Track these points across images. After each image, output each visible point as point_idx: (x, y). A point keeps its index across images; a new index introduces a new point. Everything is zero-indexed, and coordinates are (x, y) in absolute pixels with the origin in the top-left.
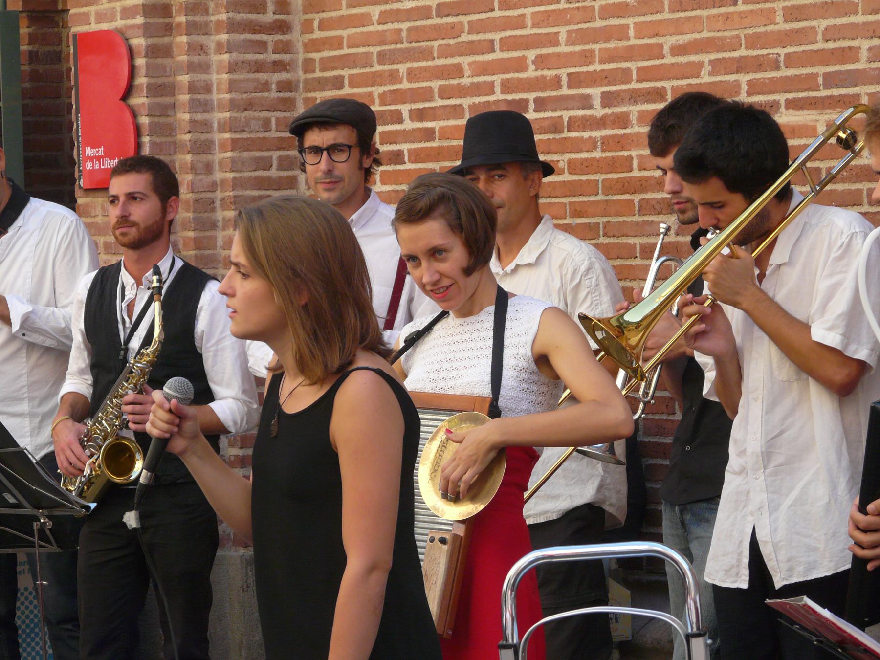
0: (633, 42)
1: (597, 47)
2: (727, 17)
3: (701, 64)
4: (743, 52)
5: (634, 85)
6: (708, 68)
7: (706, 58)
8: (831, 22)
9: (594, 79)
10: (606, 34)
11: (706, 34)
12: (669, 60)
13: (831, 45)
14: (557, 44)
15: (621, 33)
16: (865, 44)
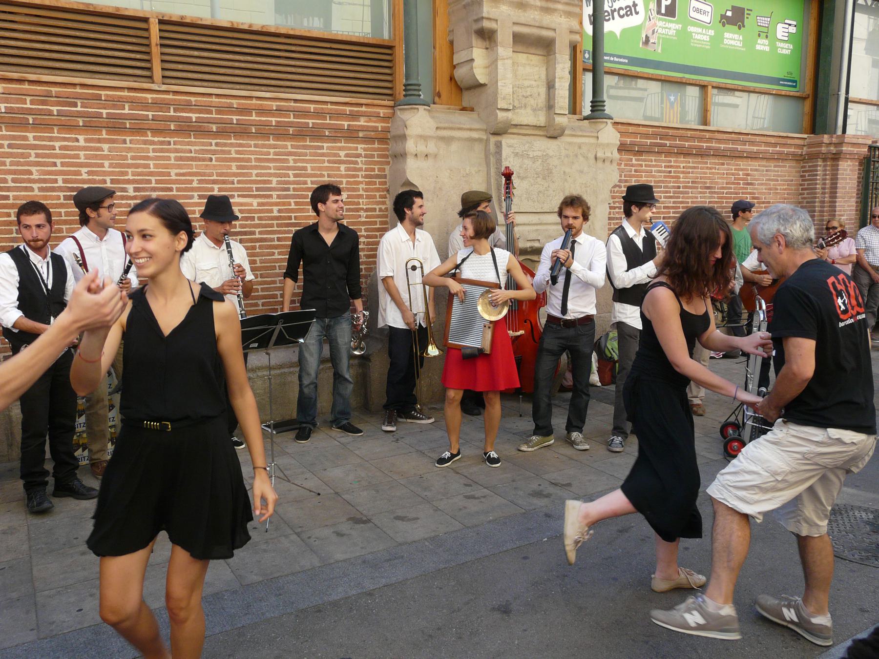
0: (152, 170)
1: (130, 170)
2: (207, 165)
3: (193, 180)
4: (215, 177)
5: (153, 185)
6: (196, 182)
7: (195, 178)
8: (259, 171)
9: (128, 182)
10: (137, 166)
11: (194, 170)
12: (174, 177)
13: (259, 178)
14: (104, 167)
15: (148, 166)
16: (275, 180)
